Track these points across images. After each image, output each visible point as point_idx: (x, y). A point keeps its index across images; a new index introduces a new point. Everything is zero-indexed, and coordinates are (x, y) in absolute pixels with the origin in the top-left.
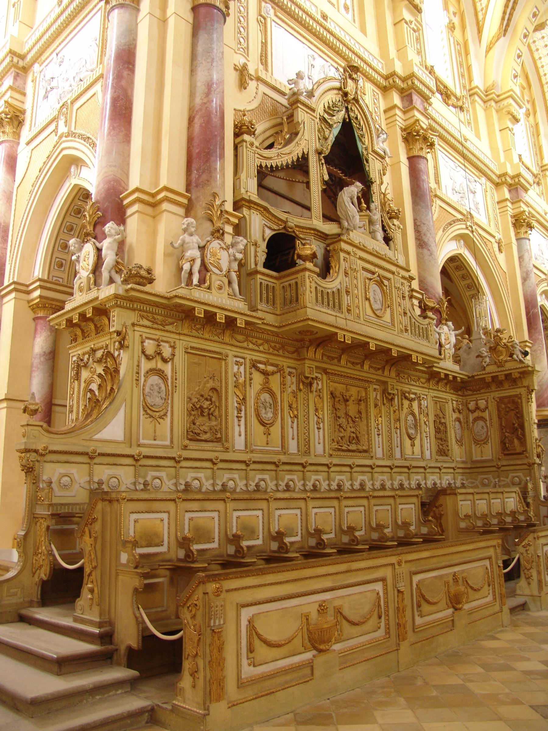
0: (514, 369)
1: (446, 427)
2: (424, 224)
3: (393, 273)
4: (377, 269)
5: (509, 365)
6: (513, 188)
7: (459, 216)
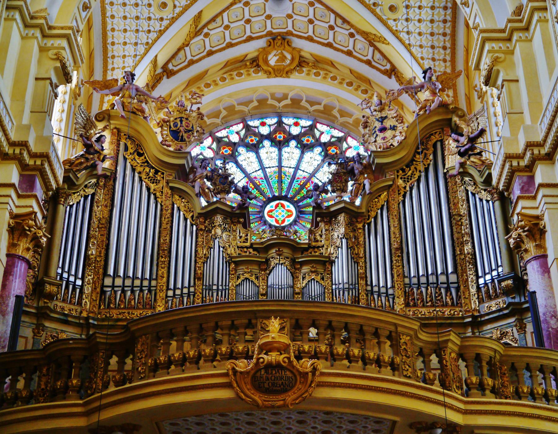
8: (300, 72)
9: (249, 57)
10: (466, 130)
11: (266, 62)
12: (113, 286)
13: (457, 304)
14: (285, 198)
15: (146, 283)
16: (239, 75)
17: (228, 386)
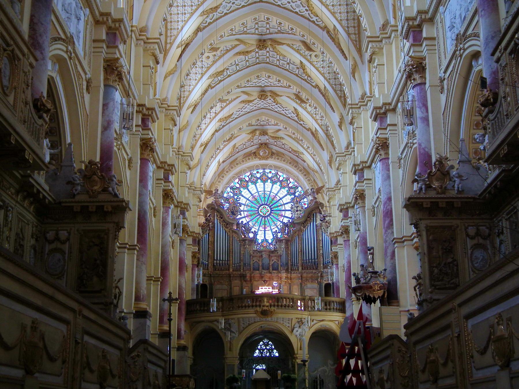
0: (108, 202)
1: (23, 251)
2: (42, 24)
3: (24, 55)
4: (12, 43)
5: (102, 197)
6: (111, 31)
7: (63, 36)
8: (272, 158)
9: (252, 152)
10: (323, 213)
11: (259, 154)
12: (217, 263)
13: (317, 269)
14: (266, 205)
15: (226, 262)
16: (249, 159)
17: (256, 313)
